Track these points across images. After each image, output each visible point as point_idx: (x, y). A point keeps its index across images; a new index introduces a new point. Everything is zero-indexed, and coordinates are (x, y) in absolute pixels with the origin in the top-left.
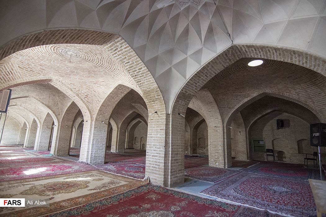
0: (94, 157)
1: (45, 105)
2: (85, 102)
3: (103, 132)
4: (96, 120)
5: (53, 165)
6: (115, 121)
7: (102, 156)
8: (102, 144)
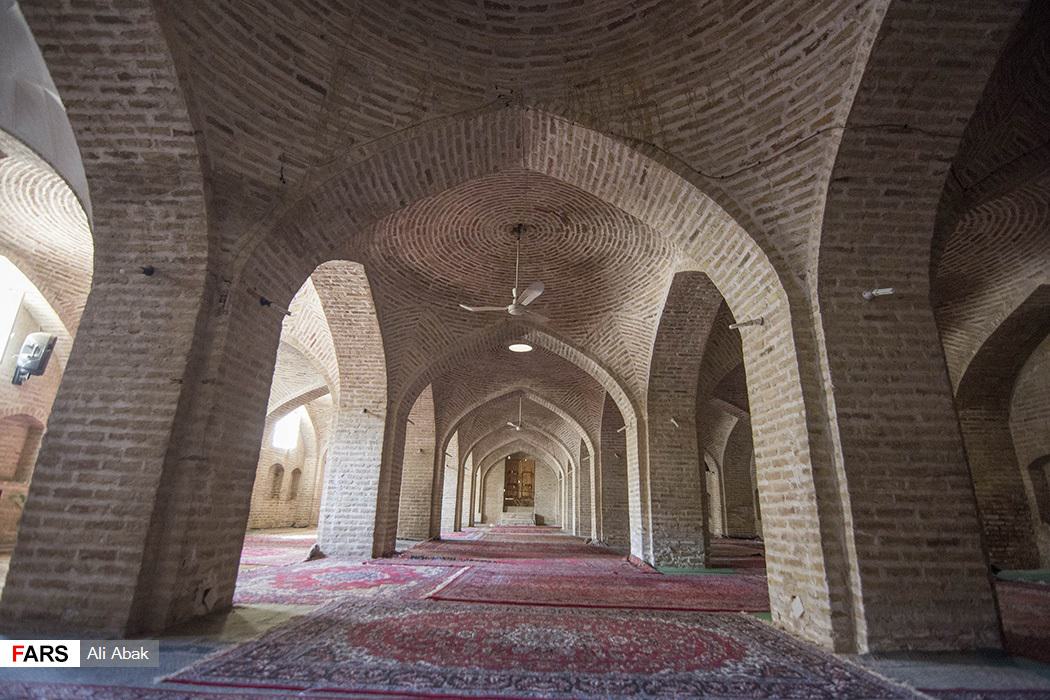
0: (335, 529)
3: (368, 445)
7: (361, 528)
8: (363, 487)
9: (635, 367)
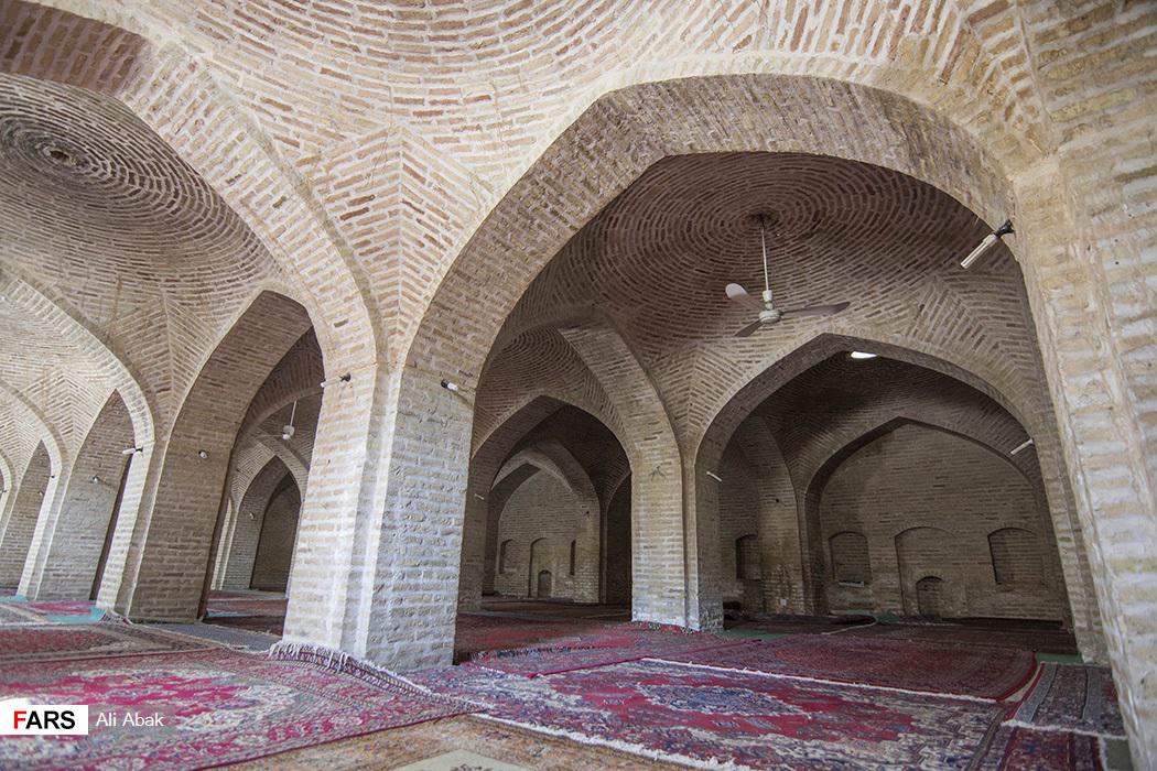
1: (93, 329)
2: (350, 243)
3: (449, 449)
4: (411, 365)
5: (90, 675)
7: (436, 610)
9: (689, 407)
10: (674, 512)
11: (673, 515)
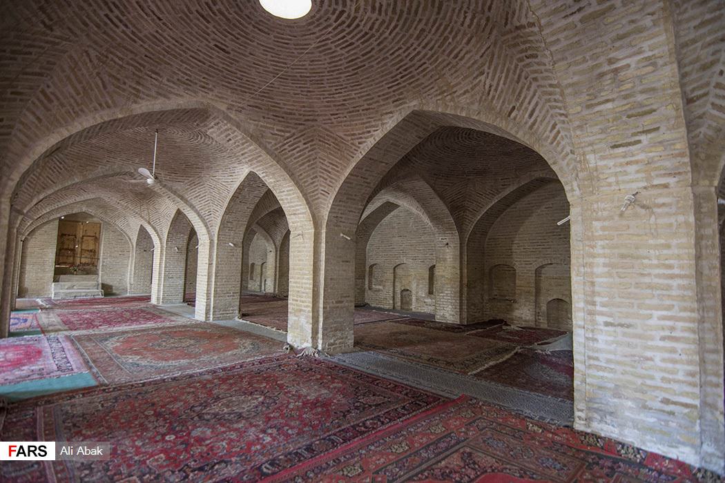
6: (297, 183)
10: (676, 271)
11: (672, 277)
